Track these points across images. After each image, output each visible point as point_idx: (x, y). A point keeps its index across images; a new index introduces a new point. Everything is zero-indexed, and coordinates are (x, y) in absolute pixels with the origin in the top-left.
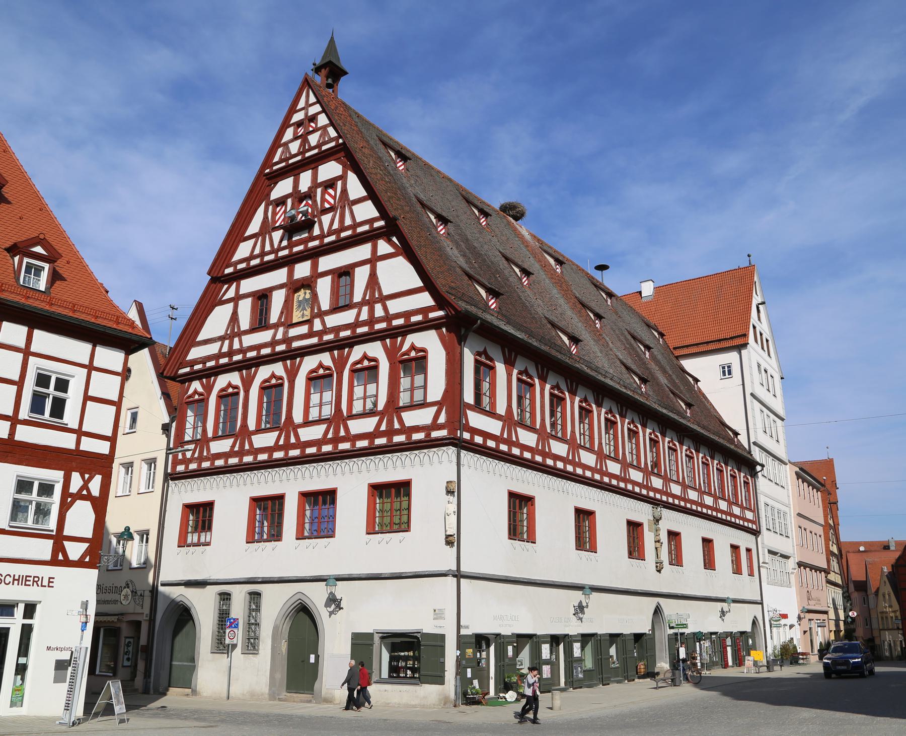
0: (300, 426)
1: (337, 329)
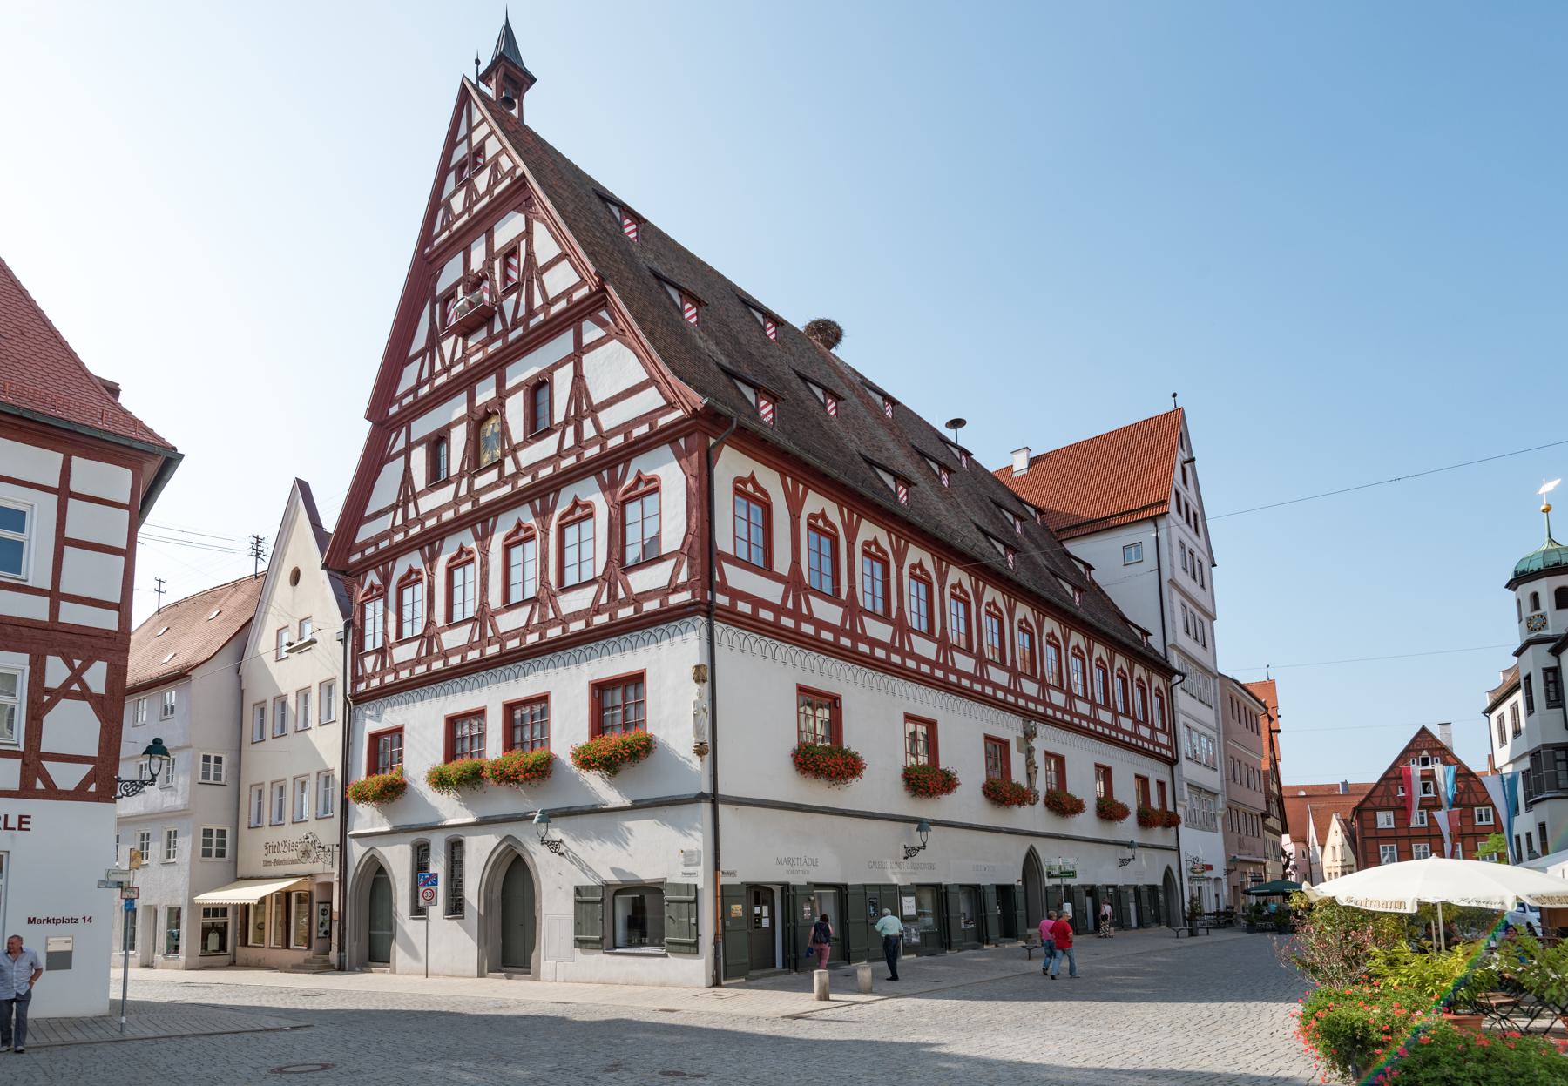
0: (499, 612)
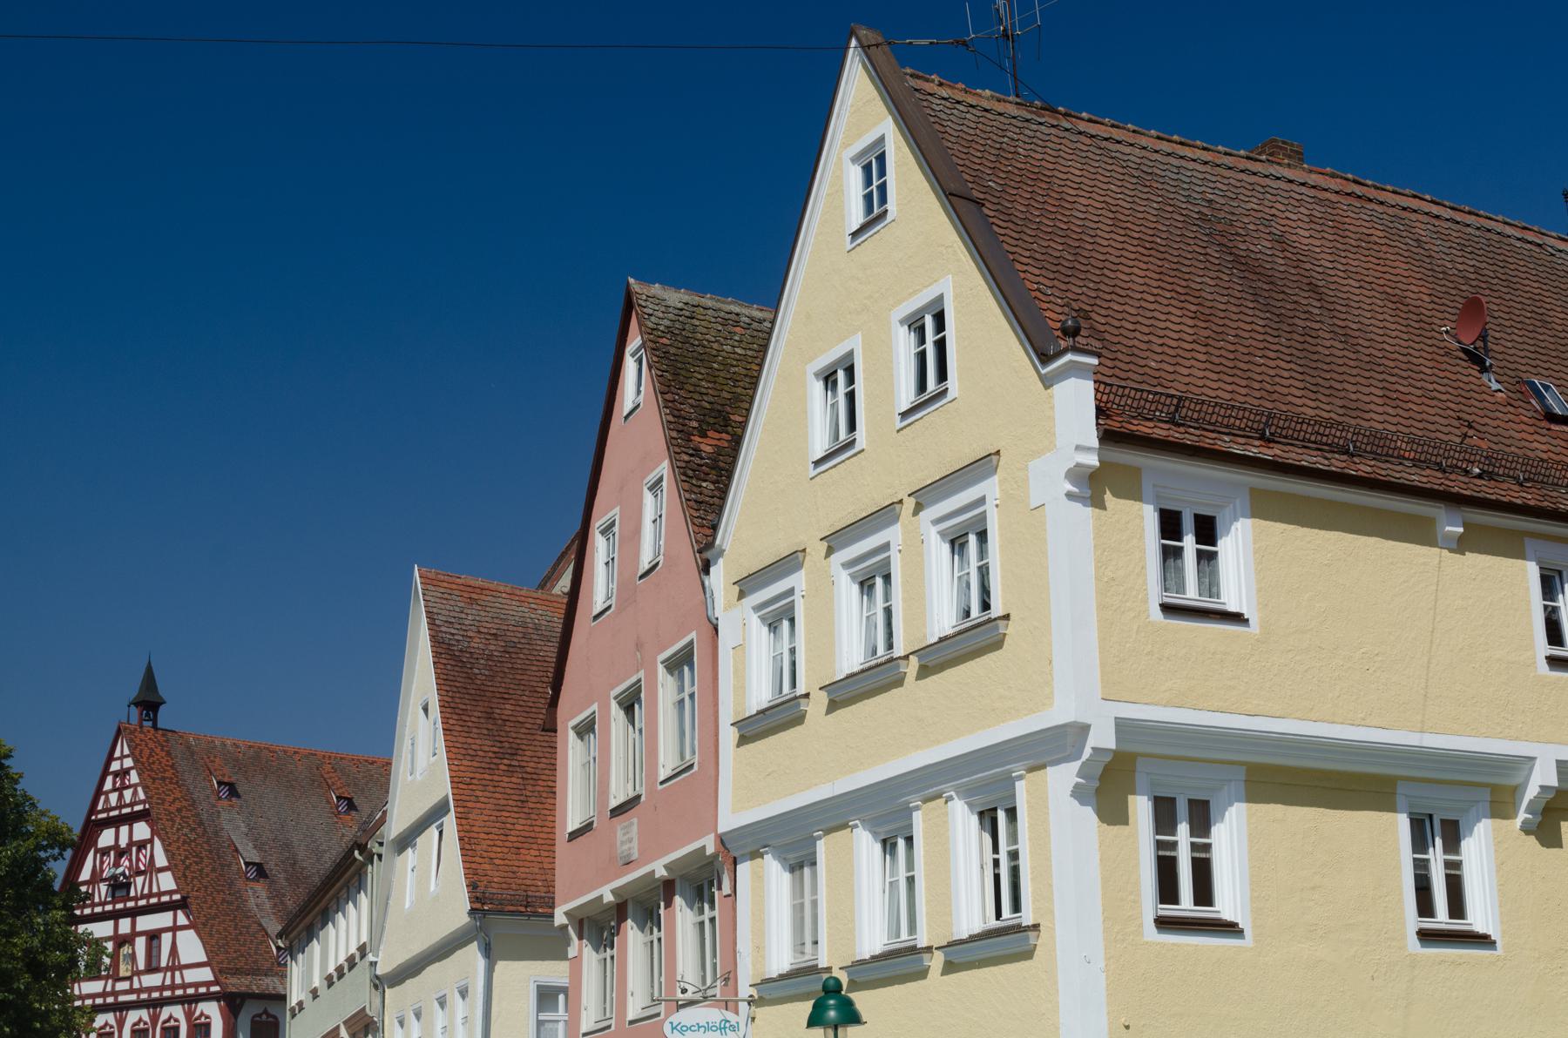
1: (150, 990)
